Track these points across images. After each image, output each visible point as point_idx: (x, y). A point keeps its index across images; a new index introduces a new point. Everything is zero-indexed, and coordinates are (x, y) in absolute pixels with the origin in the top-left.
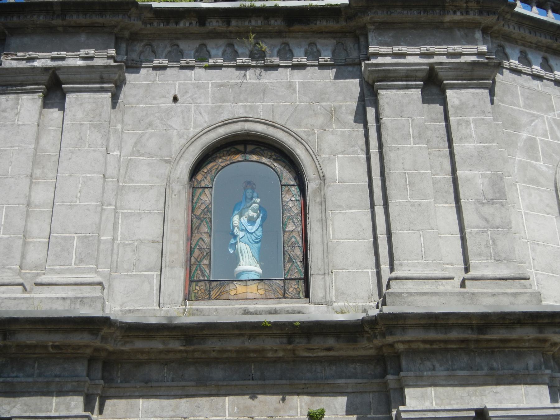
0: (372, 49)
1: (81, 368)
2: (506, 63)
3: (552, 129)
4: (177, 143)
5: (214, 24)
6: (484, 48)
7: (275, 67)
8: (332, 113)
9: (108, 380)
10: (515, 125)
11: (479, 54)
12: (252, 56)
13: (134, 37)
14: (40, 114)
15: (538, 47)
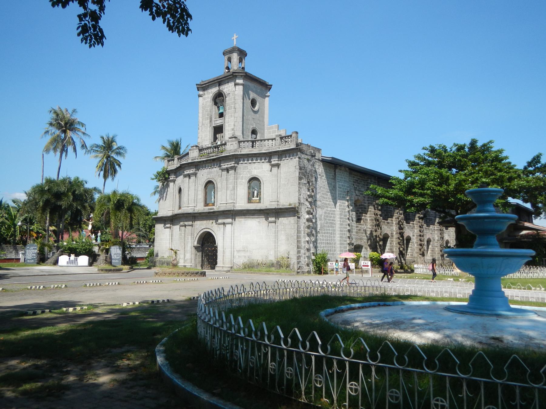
0: (221, 165)
1: (191, 218)
2: (240, 162)
3: (247, 173)
4: (203, 182)
5: (205, 162)
6: (234, 163)
7: (213, 168)
8: (219, 175)
9: (195, 219)
10: (240, 175)
11: (234, 164)
12: (211, 166)
13: (198, 165)
14: (189, 180)
15: (246, 157)
